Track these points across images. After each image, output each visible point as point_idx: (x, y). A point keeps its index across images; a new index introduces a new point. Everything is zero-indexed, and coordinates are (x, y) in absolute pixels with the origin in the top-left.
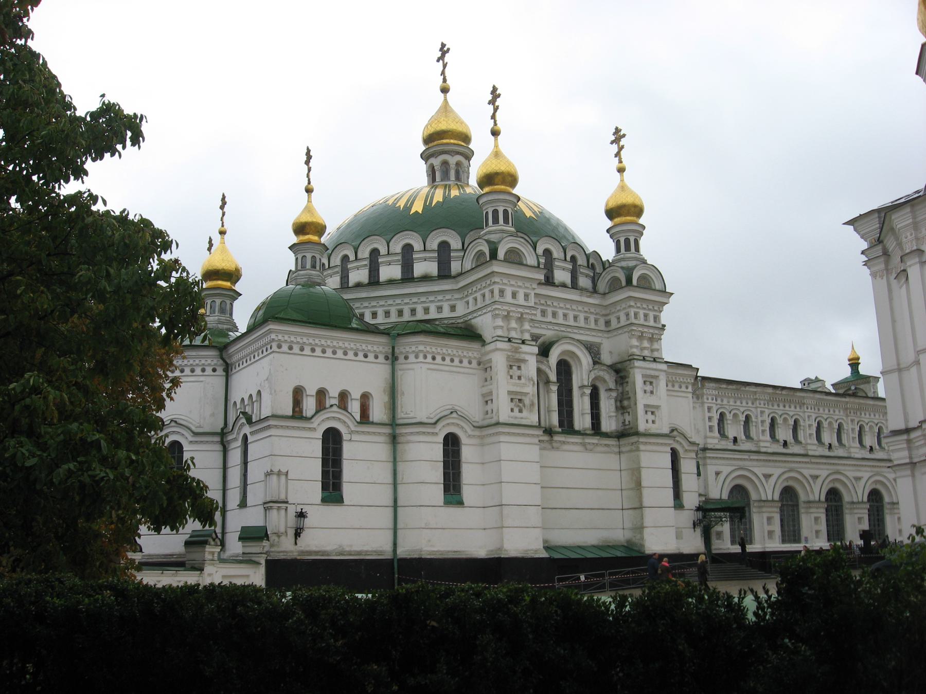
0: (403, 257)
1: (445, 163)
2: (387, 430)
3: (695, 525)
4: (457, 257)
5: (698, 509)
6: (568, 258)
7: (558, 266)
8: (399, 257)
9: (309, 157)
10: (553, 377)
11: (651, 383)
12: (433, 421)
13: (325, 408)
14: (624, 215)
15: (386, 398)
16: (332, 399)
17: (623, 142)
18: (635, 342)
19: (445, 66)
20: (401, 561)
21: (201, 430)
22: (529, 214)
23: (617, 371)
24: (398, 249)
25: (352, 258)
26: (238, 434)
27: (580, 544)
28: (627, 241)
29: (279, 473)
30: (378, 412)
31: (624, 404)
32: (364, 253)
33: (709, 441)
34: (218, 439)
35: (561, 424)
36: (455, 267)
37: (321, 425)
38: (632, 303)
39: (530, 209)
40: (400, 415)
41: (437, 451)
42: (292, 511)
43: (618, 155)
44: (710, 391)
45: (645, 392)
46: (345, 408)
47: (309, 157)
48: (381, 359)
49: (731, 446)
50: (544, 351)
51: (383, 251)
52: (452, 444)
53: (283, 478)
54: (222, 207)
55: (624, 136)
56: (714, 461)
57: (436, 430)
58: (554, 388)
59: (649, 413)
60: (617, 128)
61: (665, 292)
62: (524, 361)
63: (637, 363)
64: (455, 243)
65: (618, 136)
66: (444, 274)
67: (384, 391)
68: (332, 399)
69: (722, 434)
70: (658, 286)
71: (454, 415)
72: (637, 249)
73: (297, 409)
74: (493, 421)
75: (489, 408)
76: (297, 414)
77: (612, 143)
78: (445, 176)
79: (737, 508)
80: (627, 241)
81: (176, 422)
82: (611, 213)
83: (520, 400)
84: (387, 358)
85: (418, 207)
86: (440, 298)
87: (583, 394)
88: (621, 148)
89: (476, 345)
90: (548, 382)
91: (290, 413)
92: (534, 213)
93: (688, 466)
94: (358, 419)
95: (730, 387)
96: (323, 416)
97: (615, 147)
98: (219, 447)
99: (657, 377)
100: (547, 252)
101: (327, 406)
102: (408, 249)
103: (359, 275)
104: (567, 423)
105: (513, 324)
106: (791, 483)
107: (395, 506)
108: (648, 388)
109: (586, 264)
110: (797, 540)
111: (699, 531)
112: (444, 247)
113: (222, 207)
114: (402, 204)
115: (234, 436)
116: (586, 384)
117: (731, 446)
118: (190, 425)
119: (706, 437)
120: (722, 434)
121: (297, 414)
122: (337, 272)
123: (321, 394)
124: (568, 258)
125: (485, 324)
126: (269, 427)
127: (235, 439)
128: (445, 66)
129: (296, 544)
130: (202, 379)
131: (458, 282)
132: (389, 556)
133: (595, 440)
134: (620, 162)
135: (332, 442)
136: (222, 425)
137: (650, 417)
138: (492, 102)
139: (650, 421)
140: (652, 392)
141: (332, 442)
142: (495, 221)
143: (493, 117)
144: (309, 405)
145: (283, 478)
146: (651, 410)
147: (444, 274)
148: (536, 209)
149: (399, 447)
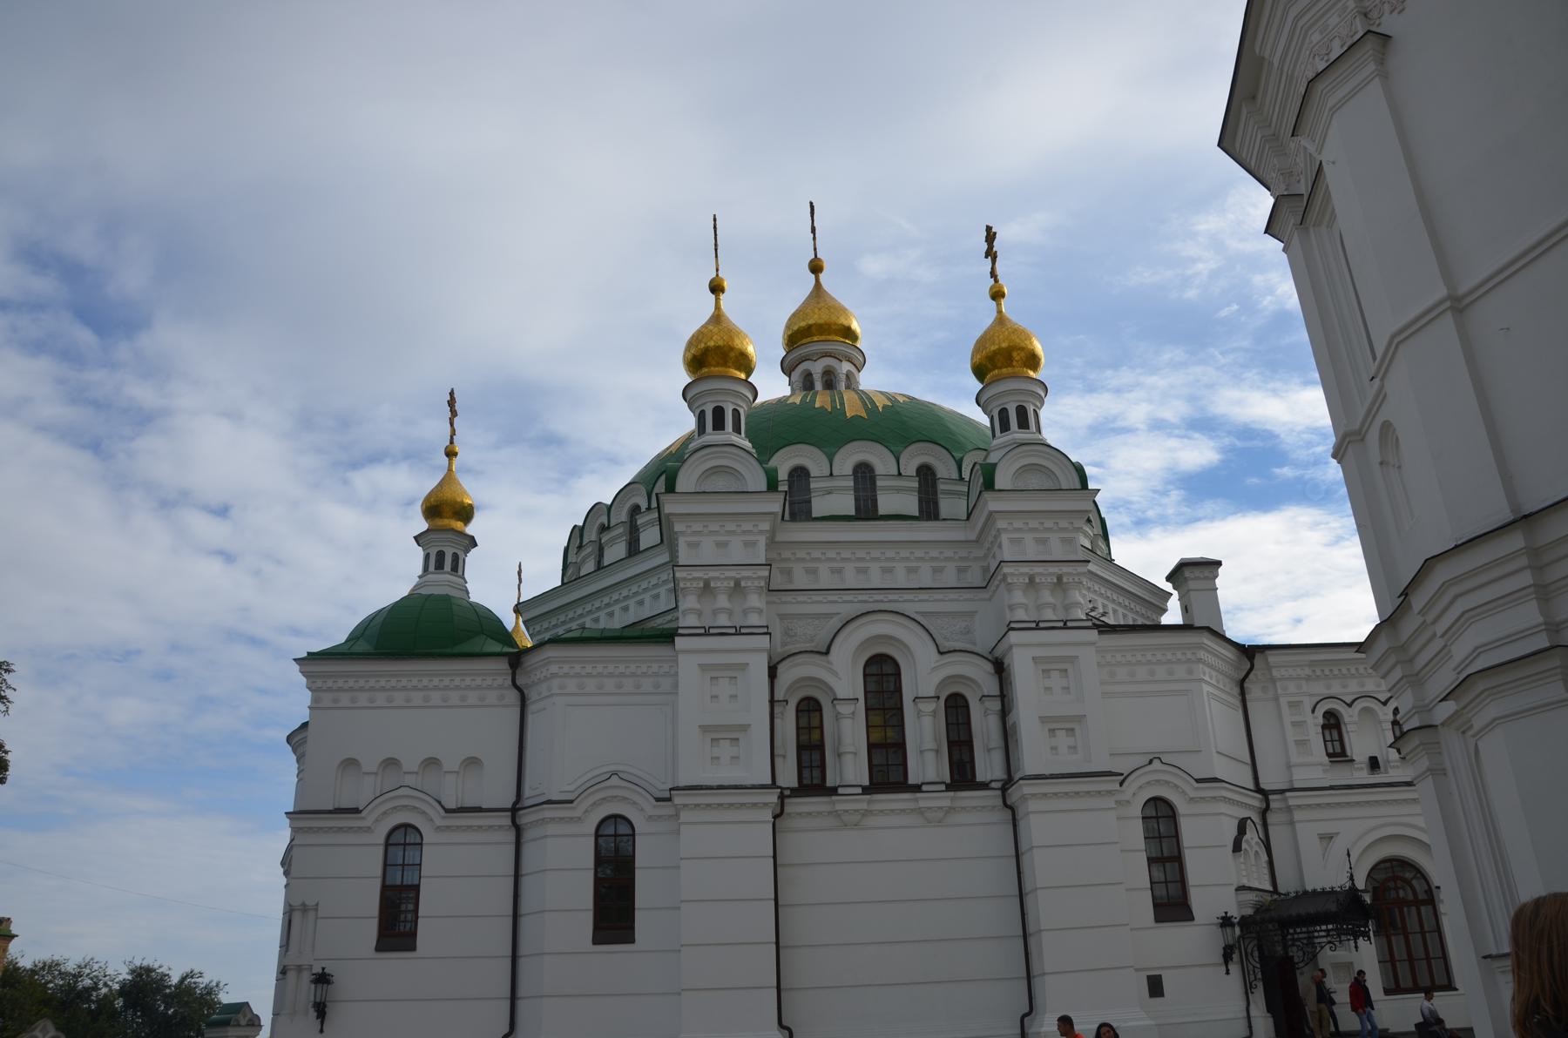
3: (1227, 956)
5: (1226, 922)
14: (1003, 362)
18: (1018, 597)
28: (1003, 413)
40: (527, 792)
63: (1014, 637)
72: (1023, 423)
82: (980, 372)
87: (919, 714)
99: (1073, 659)
104: (889, 771)
105: (723, 601)
109: (955, 475)
111: (1234, 968)
124: (910, 468)
129: (321, 1031)
133: (946, 800)
137: (1062, 740)
145: (311, 915)
146: (1063, 725)
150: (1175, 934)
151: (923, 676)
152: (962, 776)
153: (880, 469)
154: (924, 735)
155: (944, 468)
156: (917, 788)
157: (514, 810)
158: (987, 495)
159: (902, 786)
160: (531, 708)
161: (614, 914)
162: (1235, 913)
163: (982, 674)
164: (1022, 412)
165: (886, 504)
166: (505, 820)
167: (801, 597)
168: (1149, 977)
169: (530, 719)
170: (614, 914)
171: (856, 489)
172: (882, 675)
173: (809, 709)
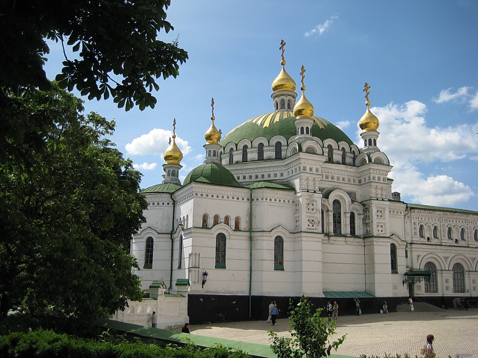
0: (259, 149)
1: (283, 100)
2: (247, 234)
4: (284, 149)
5: (406, 274)
6: (340, 149)
7: (335, 153)
8: (257, 149)
9: (213, 103)
10: (331, 208)
11: (381, 211)
13: (218, 224)
15: (248, 219)
16: (222, 219)
19: (283, 51)
20: (254, 298)
22: (321, 126)
23: (364, 205)
25: (235, 149)
26: (178, 235)
27: (343, 291)
28: (370, 140)
30: (243, 225)
31: (367, 221)
32: (241, 146)
33: (414, 239)
35: (335, 231)
36: (283, 153)
39: (323, 124)
40: (254, 226)
41: (271, 245)
42: (201, 272)
43: (366, 96)
44: (415, 214)
45: (378, 216)
46: (228, 224)
47: (213, 103)
48: (245, 200)
49: (426, 241)
50: (326, 196)
51: (249, 146)
52: (279, 242)
53: (198, 256)
54: (174, 125)
55: (370, 87)
56: (416, 250)
57: (271, 235)
58: (331, 214)
61: (389, 165)
62: (315, 201)
63: (373, 202)
64: (284, 142)
65: (367, 87)
66: (278, 157)
67: (247, 215)
68: (222, 219)
69: (422, 236)
70: (385, 162)
71: (280, 227)
72: (375, 144)
73: (205, 224)
74: (299, 230)
75: (297, 224)
76: (205, 226)
77: (364, 90)
78: (283, 107)
79: (429, 274)
80: (370, 140)
81: (150, 228)
83: (313, 220)
84: (248, 200)
86: (276, 169)
87: (346, 217)
88: (368, 94)
89: (292, 193)
90: (328, 211)
91: (201, 226)
92: (324, 126)
93: (400, 253)
94: (234, 229)
95: (426, 212)
96: (217, 227)
97: (365, 92)
98: (171, 240)
100: (330, 147)
101: (219, 222)
102: (261, 145)
103: (237, 157)
106: (459, 261)
107: (251, 271)
108: (379, 214)
109: (350, 152)
110: (463, 291)
111: (405, 285)
112: (279, 144)
113: (174, 125)
115: (177, 235)
116: (348, 212)
117: (426, 241)
118: (156, 230)
119: (412, 237)
120: (422, 236)
122: (228, 156)
123: (216, 218)
124: (340, 149)
125: (297, 183)
126: (191, 233)
127: (177, 237)
128: (283, 51)
129: (203, 288)
130: (163, 207)
131: (284, 162)
132: (247, 294)
133: (352, 239)
135: (221, 239)
136: (171, 230)
137: (380, 228)
138: (302, 74)
139: (380, 231)
140: (381, 216)
141: (221, 239)
143: (302, 81)
144: (211, 222)
147: (278, 157)
148: (326, 124)
149: (253, 242)
150: (395, 275)
151: (347, 207)
153: (334, 147)
154: (345, 221)
159: (341, 235)
163: (360, 208)
164: (375, 141)
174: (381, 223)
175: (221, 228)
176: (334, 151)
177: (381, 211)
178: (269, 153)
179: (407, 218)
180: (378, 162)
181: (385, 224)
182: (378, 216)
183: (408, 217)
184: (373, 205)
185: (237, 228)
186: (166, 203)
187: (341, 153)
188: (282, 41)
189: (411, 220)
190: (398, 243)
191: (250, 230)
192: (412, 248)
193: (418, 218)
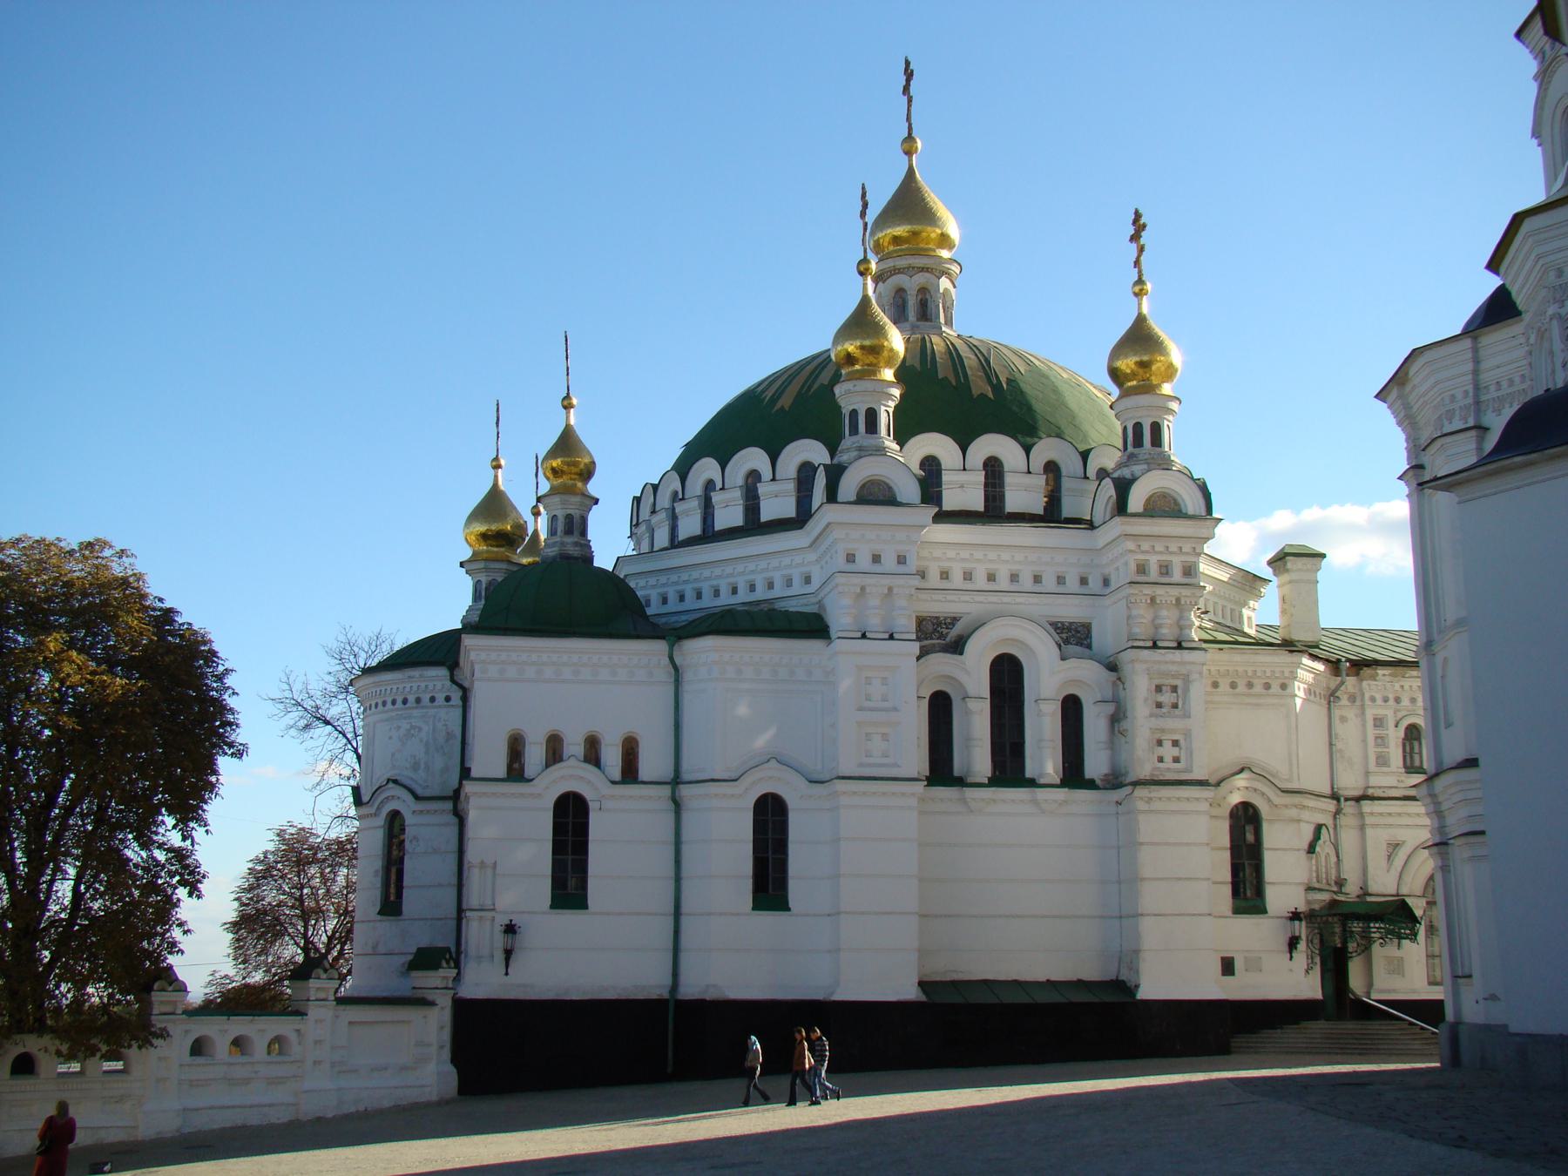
3: (1293, 943)
5: (1295, 916)
12: (733, 776)
16: (574, 746)
17: (1145, 237)
21: (428, 793)
22: (980, 387)
24: (740, 481)
28: (1138, 427)
29: (483, 865)
30: (653, 763)
33: (1374, 781)
34: (449, 805)
37: (551, 785)
38: (1131, 545)
41: (743, 827)
51: (719, 485)
53: (489, 872)
59: (1167, 744)
60: (1137, 212)
68: (574, 746)
73: (516, 766)
76: (516, 771)
80: (1138, 427)
85: (786, 401)
88: (1141, 250)
89: (815, 645)
91: (502, 772)
92: (997, 388)
94: (617, 775)
96: (557, 770)
97: (1134, 246)
98: (456, 820)
104: (1009, 766)
108: (1167, 698)
114: (769, 394)
119: (1367, 773)
121: (516, 771)
132: (666, 995)
133: (1063, 793)
134: (1140, 281)
137: (1168, 751)
139: (1168, 759)
140: (1175, 706)
142: (854, 430)
144: (534, 755)
150: (1247, 922)
152: (1073, 775)
155: (1070, 464)
156: (1032, 783)
157: (676, 781)
158: (1117, 519)
160: (687, 688)
161: (770, 886)
162: (1302, 908)
164: (1156, 429)
165: (1013, 502)
166: (666, 791)
167: (938, 596)
168: (1223, 959)
169: (687, 699)
170: (770, 886)
171: (986, 485)
172: (1007, 676)
173: (940, 708)
174: (1173, 731)
175: (573, 776)
176: (1009, 479)
177: (1174, 689)
178: (777, 502)
179: (1344, 701)
180: (1164, 507)
181: (1187, 734)
182: (1159, 705)
183: (1352, 699)
184: (1139, 667)
185: (630, 772)
186: (440, 697)
187: (1040, 481)
188: (907, 63)
189: (1362, 707)
190: (1269, 800)
191: (676, 781)
192: (1361, 815)
193: (1397, 700)
